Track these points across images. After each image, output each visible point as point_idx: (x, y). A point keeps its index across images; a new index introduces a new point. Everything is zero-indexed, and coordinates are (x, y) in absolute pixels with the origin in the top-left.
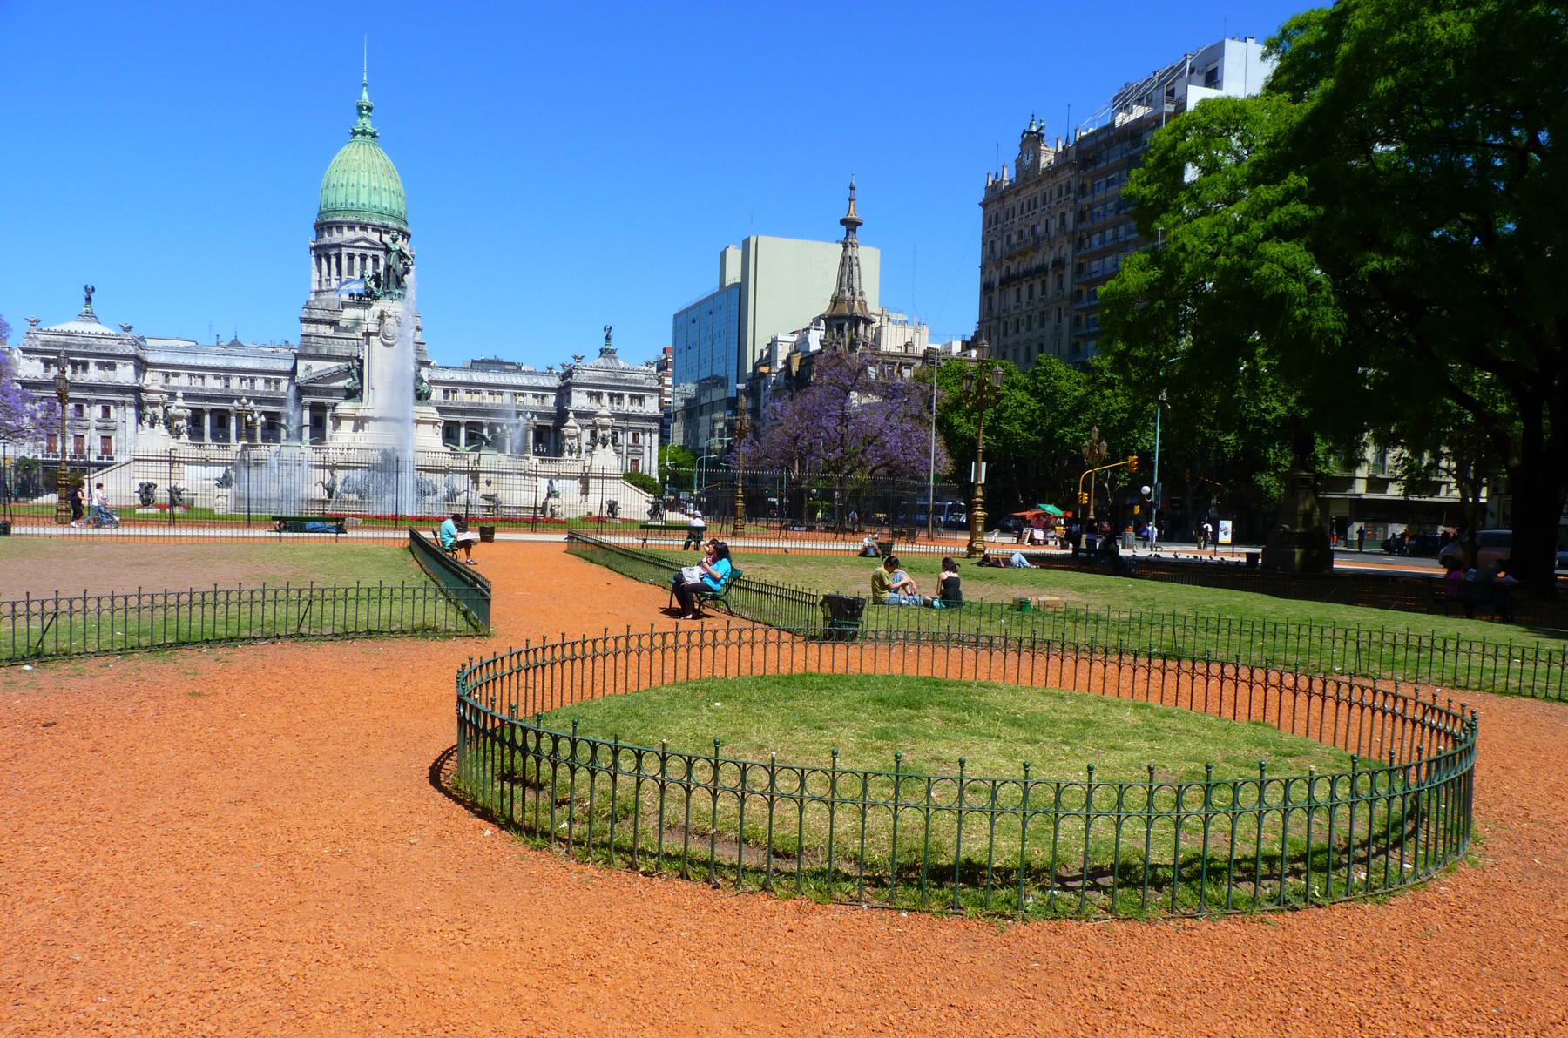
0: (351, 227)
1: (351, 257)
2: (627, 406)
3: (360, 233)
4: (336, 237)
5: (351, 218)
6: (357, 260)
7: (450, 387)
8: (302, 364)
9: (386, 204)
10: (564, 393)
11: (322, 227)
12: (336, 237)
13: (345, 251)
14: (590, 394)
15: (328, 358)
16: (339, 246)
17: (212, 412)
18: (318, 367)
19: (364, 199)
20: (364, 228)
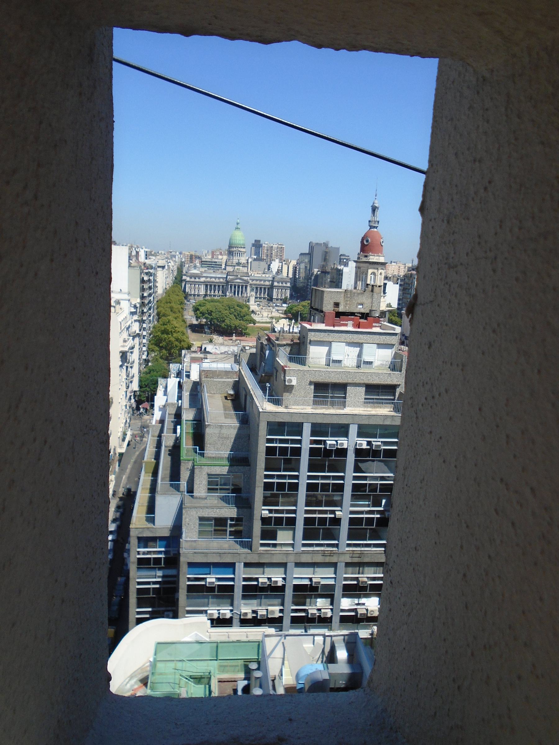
0: (235, 247)
1: (235, 253)
2: (284, 285)
3: (237, 249)
4: (232, 250)
5: (235, 246)
6: (236, 254)
7: (253, 280)
8: (228, 277)
9: (242, 243)
10: (273, 281)
11: (230, 247)
12: (232, 250)
13: (234, 252)
14: (277, 283)
15: (233, 276)
16: (233, 251)
17: (214, 285)
18: (231, 277)
19: (238, 242)
20: (238, 248)
